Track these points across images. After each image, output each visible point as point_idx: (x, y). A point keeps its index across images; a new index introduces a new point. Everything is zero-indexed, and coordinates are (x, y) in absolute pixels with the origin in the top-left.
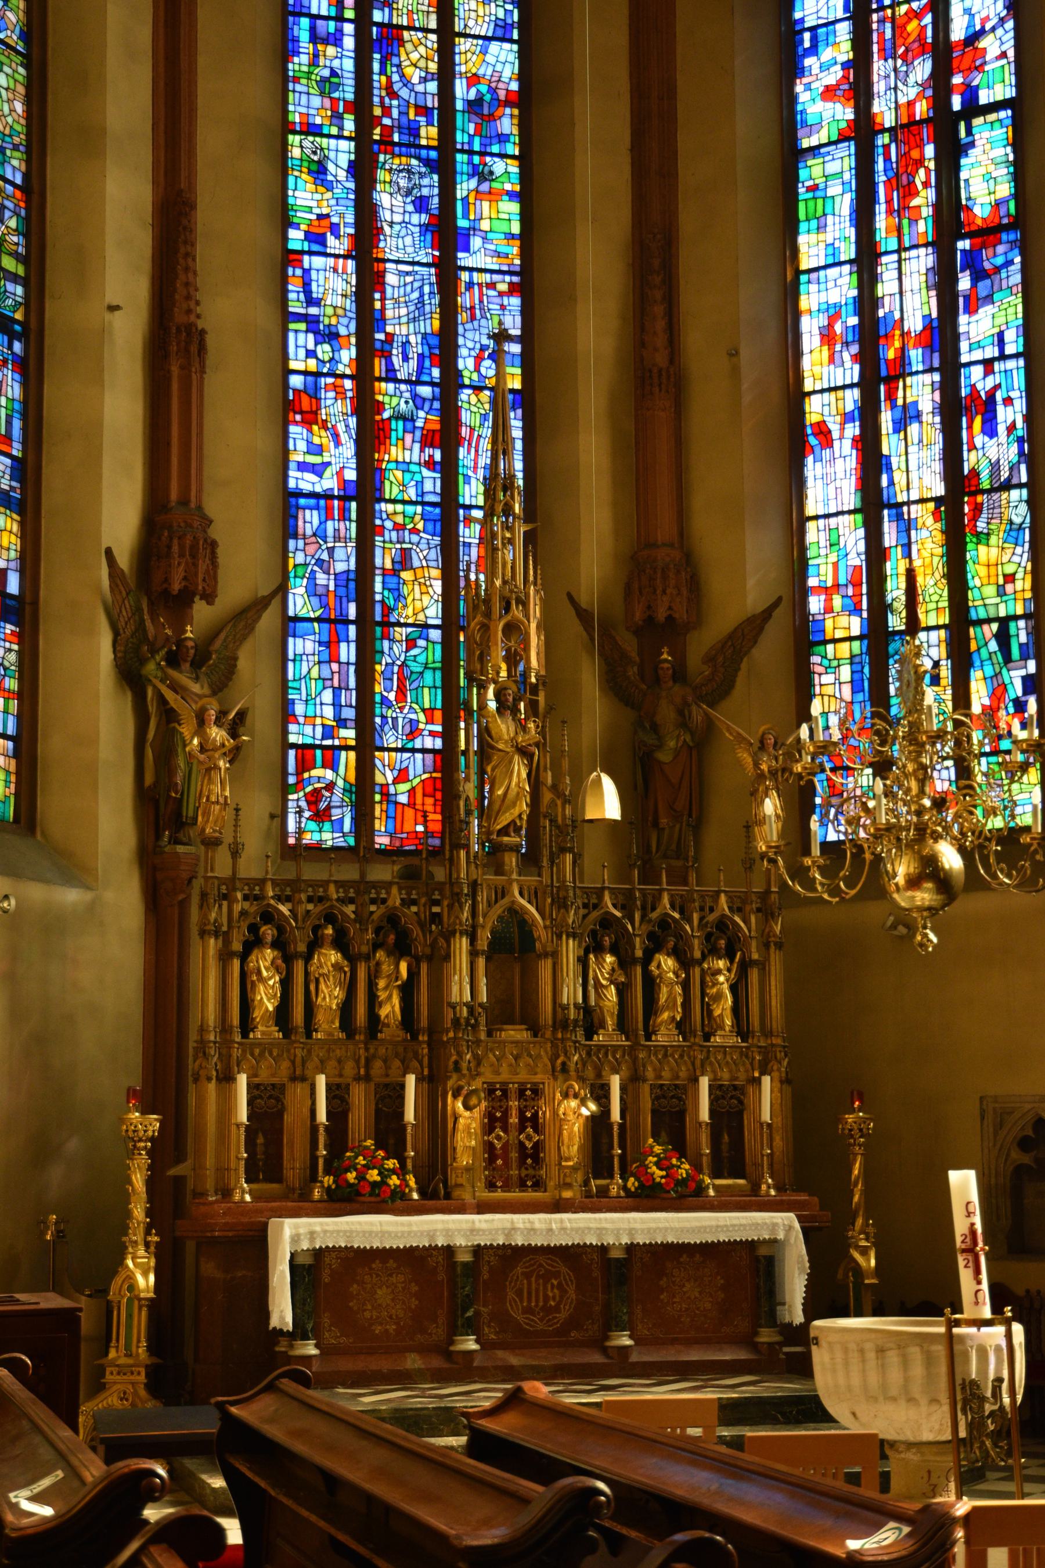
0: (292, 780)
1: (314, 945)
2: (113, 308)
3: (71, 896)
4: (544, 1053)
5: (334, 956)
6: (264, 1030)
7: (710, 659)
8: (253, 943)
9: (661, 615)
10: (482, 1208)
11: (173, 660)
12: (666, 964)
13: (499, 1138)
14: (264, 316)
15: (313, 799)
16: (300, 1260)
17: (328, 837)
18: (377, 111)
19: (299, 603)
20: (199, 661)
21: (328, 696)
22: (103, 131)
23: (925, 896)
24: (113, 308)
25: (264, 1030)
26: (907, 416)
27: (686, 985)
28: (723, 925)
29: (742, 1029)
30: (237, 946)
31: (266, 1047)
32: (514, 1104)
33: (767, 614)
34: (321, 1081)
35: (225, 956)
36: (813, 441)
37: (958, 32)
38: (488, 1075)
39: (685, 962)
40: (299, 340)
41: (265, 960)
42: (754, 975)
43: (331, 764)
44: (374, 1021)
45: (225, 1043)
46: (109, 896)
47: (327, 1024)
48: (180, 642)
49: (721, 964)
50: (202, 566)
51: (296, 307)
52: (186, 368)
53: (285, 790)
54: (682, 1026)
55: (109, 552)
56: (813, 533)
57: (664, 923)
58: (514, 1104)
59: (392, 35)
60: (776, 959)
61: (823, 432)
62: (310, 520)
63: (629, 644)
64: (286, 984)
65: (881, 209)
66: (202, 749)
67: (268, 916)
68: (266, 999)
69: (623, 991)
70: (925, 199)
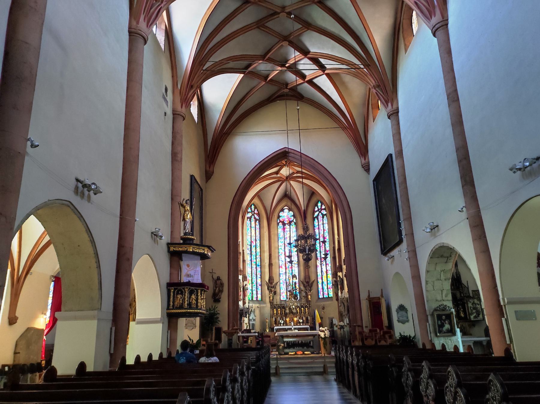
0: (281, 295)
1: (278, 309)
3: (264, 305)
4: (293, 316)
5: (279, 309)
6: (275, 314)
7: (311, 284)
8: (274, 309)
9: (306, 281)
10: (289, 326)
11: (271, 288)
12: (302, 309)
13: (290, 321)
14: (277, 261)
15: (283, 296)
16: (276, 329)
17: (284, 299)
18: (285, 244)
19: (281, 281)
20: (273, 287)
21: (284, 288)
22: (265, 251)
23: (293, 309)
25: (275, 314)
26: (323, 265)
27: (304, 310)
28: (307, 306)
29: (308, 313)
30: (273, 309)
31: (275, 315)
32: (291, 319)
33: (314, 281)
34: (279, 318)
35: (272, 310)
36: (318, 266)
37: (325, 236)
38: (289, 317)
39: (304, 308)
40: (280, 262)
41: (275, 310)
42: (309, 309)
43: (284, 293)
44: (282, 314)
45: (273, 315)
46: (267, 305)
47: (279, 314)
48: (271, 286)
49: (306, 308)
50: (273, 281)
51: (280, 259)
52: (271, 266)
53: (281, 296)
54: (304, 313)
56: (318, 274)
57: (302, 306)
58: (291, 319)
59: (287, 238)
60: (310, 308)
61: (318, 266)
62: (281, 275)
63: (305, 283)
64: (276, 311)
65: (321, 249)
67: (275, 307)
68: (275, 312)
69: (300, 311)
70: (324, 248)
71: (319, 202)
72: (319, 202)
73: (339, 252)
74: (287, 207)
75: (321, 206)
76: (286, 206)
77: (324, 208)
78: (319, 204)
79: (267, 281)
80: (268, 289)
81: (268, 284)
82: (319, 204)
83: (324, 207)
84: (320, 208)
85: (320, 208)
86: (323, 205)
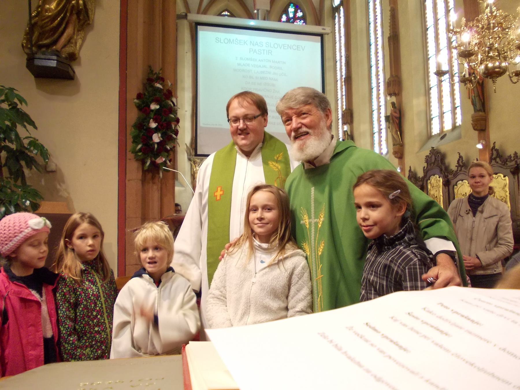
2: (186, 111)
24: (186, 111)
55: (186, 144)
66: (196, 170)
71: (292, 5)
72: (292, 5)
73: (348, 84)
74: (228, 12)
75: (295, 12)
76: (226, 10)
77: (300, 16)
78: (291, 10)
79: (188, 145)
80: (190, 160)
81: (190, 151)
82: (291, 10)
83: (301, 13)
84: (291, 15)
85: (291, 15)
86: (299, 11)
